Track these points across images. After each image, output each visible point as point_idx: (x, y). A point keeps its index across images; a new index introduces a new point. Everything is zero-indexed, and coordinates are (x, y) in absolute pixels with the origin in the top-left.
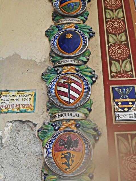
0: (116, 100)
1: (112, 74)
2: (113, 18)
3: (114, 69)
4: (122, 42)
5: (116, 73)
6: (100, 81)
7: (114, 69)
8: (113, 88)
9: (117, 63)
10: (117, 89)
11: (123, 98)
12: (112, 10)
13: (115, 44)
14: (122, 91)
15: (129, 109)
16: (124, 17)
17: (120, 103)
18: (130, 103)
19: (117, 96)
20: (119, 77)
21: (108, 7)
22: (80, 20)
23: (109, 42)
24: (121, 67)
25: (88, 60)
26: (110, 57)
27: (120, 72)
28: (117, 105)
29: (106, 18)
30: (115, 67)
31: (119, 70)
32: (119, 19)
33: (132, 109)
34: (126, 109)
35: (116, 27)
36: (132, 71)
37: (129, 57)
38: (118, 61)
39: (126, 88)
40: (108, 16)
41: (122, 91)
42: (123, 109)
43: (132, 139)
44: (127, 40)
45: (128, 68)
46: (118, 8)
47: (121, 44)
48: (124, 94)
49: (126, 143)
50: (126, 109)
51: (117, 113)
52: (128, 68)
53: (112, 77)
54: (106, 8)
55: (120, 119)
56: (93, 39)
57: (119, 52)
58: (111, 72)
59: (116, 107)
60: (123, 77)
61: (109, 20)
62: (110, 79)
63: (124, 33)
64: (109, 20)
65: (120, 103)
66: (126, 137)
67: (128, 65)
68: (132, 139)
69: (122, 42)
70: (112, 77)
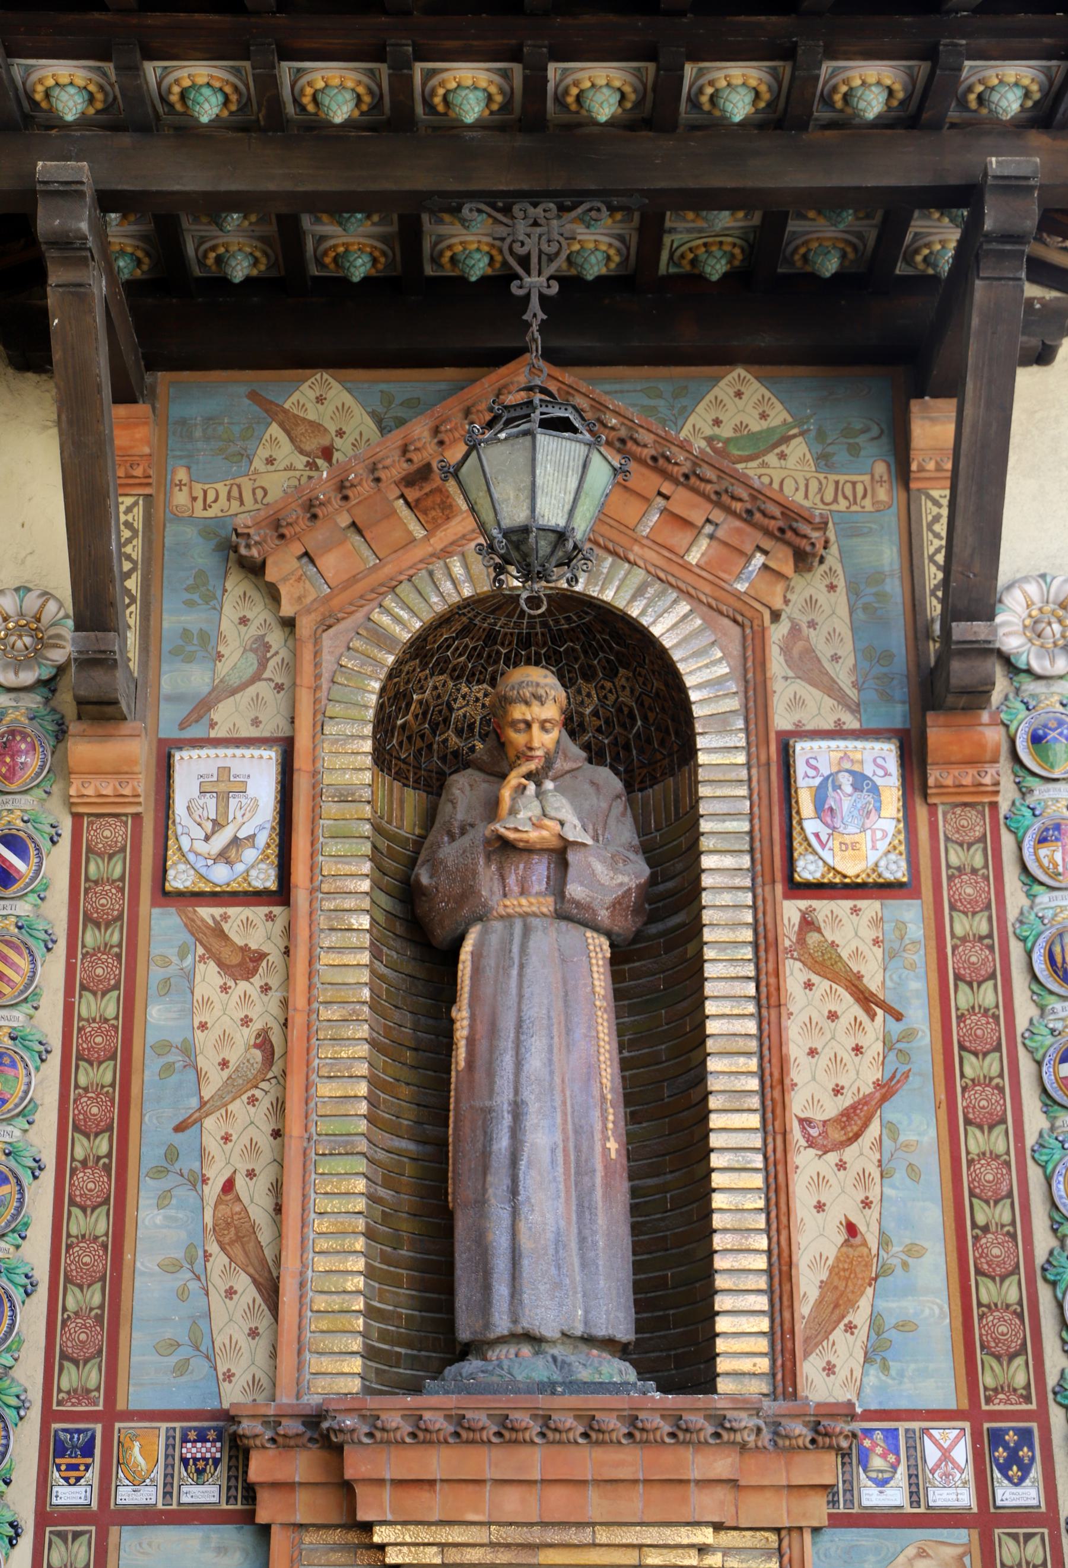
0: (58, 1461)
1: (62, 1395)
2: (83, 1236)
3: (65, 1385)
4: (91, 1309)
5: (68, 1393)
6: (35, 1414)
7: (65, 1385)
8: (56, 1431)
9: (72, 1368)
10: (62, 1435)
11: (70, 1457)
12: (84, 1209)
13: (76, 1313)
14: (72, 1439)
15: (78, 1479)
16: (106, 1234)
17: (63, 1467)
18: (82, 1468)
19: (61, 1450)
20: (73, 1405)
21: (78, 1199)
22: (7, 1246)
23: (64, 1309)
24: (80, 1378)
25: (16, 1360)
26: (61, 1351)
27: (75, 1391)
28: (59, 1470)
29: (69, 1236)
30: (69, 1378)
31: (75, 1385)
32: (96, 1238)
33: (82, 1481)
34: (72, 1481)
35: (85, 1264)
36: (98, 1389)
37: (100, 1351)
38: (76, 1363)
39: (79, 1431)
40: (74, 1231)
41: (72, 1439)
42: (66, 1479)
43: (73, 1540)
44: (101, 1307)
45: (92, 1383)
46: (100, 1205)
47: (89, 1317)
48: (74, 1447)
49: (63, 1548)
50: (72, 1481)
51: (55, 1489)
52: (92, 1383)
53: (59, 1403)
54: (72, 1203)
55: (59, 1502)
56: (34, 1297)
57: (83, 1337)
58: (60, 1391)
59: (56, 1474)
60: (80, 1404)
61: (75, 1240)
62: (55, 1407)
63: (98, 1285)
64: (75, 1240)
65: (63, 1467)
66: (62, 1536)
67: (94, 1374)
68: (73, 1540)
69: (91, 1309)
70: (59, 1403)
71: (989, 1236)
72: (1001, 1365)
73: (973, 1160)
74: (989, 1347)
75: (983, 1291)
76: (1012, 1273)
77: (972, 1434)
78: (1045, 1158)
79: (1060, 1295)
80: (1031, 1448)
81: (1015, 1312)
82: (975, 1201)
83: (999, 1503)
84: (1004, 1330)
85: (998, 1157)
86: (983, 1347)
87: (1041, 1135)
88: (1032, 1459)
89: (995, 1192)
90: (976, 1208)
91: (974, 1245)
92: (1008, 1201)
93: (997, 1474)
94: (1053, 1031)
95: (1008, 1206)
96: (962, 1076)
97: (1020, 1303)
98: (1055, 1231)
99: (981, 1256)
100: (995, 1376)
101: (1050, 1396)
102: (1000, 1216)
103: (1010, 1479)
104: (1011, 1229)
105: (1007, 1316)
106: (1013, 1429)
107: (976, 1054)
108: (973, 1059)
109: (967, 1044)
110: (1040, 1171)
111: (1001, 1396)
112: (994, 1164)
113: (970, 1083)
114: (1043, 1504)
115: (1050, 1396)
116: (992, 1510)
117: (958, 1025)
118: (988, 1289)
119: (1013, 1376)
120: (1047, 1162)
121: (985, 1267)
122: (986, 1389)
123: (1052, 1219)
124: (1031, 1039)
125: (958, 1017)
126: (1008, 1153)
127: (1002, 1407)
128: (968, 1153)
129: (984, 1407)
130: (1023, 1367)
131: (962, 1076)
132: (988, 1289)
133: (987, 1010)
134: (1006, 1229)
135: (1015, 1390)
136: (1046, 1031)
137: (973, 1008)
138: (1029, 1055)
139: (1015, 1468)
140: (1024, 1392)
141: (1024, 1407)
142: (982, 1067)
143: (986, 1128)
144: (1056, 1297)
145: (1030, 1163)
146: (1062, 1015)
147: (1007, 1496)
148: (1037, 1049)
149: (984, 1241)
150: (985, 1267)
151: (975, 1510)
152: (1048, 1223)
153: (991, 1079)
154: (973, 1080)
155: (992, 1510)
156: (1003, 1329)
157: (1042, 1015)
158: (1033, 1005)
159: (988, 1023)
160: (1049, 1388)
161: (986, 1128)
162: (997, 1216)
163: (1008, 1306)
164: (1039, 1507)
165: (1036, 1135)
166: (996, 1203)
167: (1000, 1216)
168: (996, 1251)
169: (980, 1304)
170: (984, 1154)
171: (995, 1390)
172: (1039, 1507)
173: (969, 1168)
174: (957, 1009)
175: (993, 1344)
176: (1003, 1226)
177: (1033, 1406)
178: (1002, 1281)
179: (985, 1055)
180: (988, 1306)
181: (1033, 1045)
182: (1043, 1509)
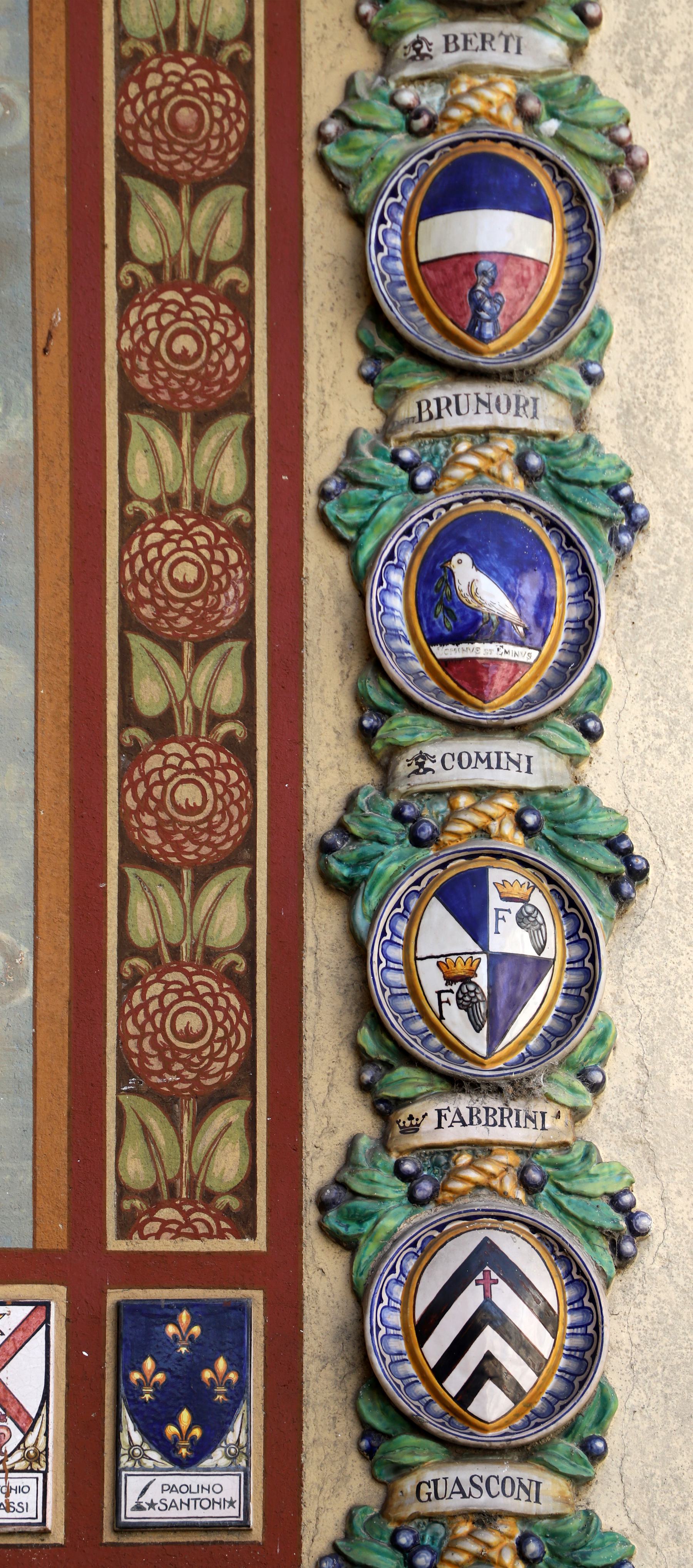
71: (173, 748)
72: (175, 1123)
73: (140, 518)
74: (144, 1073)
75: (139, 908)
76: (229, 861)
77: (71, 1321)
78: (354, 516)
79: (362, 922)
80: (240, 1363)
81: (229, 973)
82: (137, 642)
83: (129, 1515)
84: (196, 1024)
85: (217, 511)
86: (124, 1073)
87: (351, 448)
88: (239, 1393)
89: (199, 618)
90: (140, 663)
91: (124, 773)
92: (239, 646)
93: (132, 1434)
94: (411, 113)
95: (235, 662)
96: (125, 253)
97: (247, 947)
98: (366, 735)
99: (143, 807)
100: (154, 1155)
101: (311, 1214)
102: (211, 688)
103: (167, 1449)
104: (237, 728)
105: (205, 983)
106: (189, 1305)
107: (171, 188)
108: (162, 202)
109: (147, 153)
110: (338, 559)
111: (166, 1213)
112: (203, 534)
113: (147, 278)
114: (256, 1520)
115: (311, 1214)
116: (108, 1537)
117: (121, 90)
118: (154, 904)
119: (209, 1155)
120: (360, 529)
121: (154, 838)
122: (123, 1191)
123: (361, 701)
124: (342, 141)
125: (121, 62)
126: (247, 501)
127: (166, 1244)
128: (126, 495)
129: (114, 1244)
130: (238, 1133)
131: (125, 253)
132: (154, 904)
133: (214, 45)
134: (224, 729)
135: (209, 1196)
136: (390, 118)
137: (172, 34)
138: (334, 197)
139: (185, 1417)
140: (235, 1204)
141: (232, 1244)
142: (186, 230)
143: (187, 419)
144: (351, 930)
145: (312, 531)
146: (443, 61)
147: (154, 1494)
148: (357, 174)
149: (155, 762)
150: (154, 838)
151: (58, 1536)
152: (348, 713)
153: (214, 268)
154: (156, 269)
155: (108, 1537)
156: (191, 1021)
157: (384, 71)
158: (358, 36)
159: (216, 87)
160: (310, 1191)
161: (187, 419)
162: (199, 690)
163: (211, 954)
164: (243, 1526)
165: (337, 450)
166: (201, 650)
167: (211, 688)
168: (188, 794)
169: (127, 949)
170: (175, 500)
171: (152, 1197)
172: (243, 1526)
173: (125, 543)
174: (122, 35)
175: (156, 1064)
176: (215, 720)
177: (259, 1244)
178: (199, 884)
179: (200, 190)
180: (151, 955)
181: (348, 160)
182: (257, 1534)
